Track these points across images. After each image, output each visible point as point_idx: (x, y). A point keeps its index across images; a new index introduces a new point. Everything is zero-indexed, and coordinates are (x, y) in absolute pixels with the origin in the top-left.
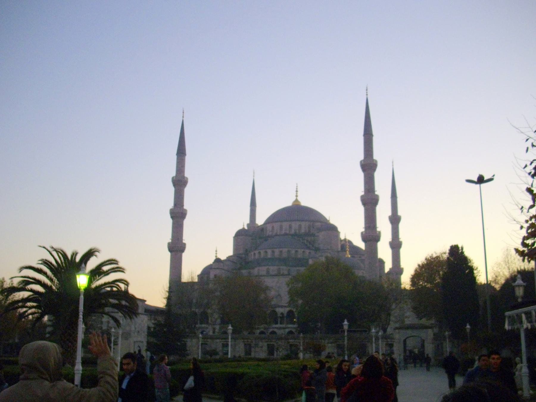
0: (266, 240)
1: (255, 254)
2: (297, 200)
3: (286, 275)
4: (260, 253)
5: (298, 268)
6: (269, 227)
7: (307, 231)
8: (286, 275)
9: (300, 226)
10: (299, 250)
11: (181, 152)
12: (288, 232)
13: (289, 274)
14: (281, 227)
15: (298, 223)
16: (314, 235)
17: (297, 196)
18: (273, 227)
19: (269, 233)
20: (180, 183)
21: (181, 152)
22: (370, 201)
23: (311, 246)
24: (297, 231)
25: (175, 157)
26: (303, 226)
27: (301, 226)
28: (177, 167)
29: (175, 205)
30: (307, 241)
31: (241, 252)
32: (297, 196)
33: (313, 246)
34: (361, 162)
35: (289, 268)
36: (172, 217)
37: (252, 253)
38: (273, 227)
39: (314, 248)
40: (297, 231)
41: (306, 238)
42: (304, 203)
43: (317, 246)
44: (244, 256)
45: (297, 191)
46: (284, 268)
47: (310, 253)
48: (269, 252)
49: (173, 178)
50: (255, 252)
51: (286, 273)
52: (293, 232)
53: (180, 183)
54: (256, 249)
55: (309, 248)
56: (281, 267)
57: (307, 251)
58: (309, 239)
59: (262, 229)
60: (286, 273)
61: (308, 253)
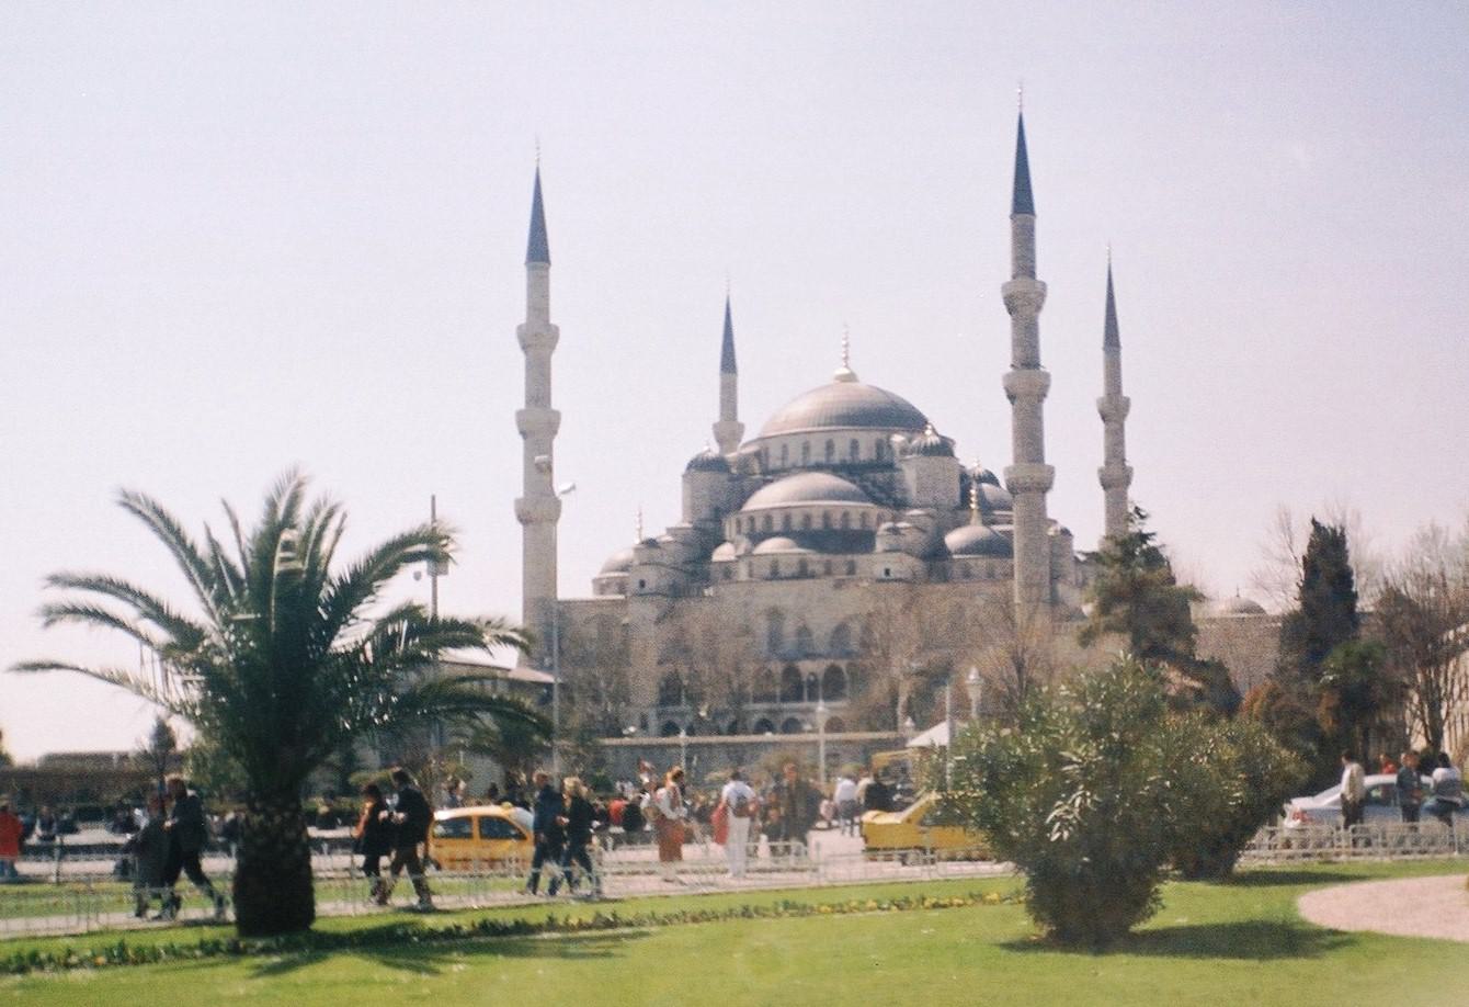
5: (849, 557)
7: (874, 456)
12: (822, 459)
16: (890, 466)
20: (538, 340)
22: (1027, 389)
23: (883, 496)
28: (530, 296)
30: (874, 483)
31: (705, 513)
33: (889, 497)
36: (524, 433)
39: (892, 502)
41: (871, 475)
43: (899, 496)
49: (520, 328)
53: (538, 340)
58: (880, 477)
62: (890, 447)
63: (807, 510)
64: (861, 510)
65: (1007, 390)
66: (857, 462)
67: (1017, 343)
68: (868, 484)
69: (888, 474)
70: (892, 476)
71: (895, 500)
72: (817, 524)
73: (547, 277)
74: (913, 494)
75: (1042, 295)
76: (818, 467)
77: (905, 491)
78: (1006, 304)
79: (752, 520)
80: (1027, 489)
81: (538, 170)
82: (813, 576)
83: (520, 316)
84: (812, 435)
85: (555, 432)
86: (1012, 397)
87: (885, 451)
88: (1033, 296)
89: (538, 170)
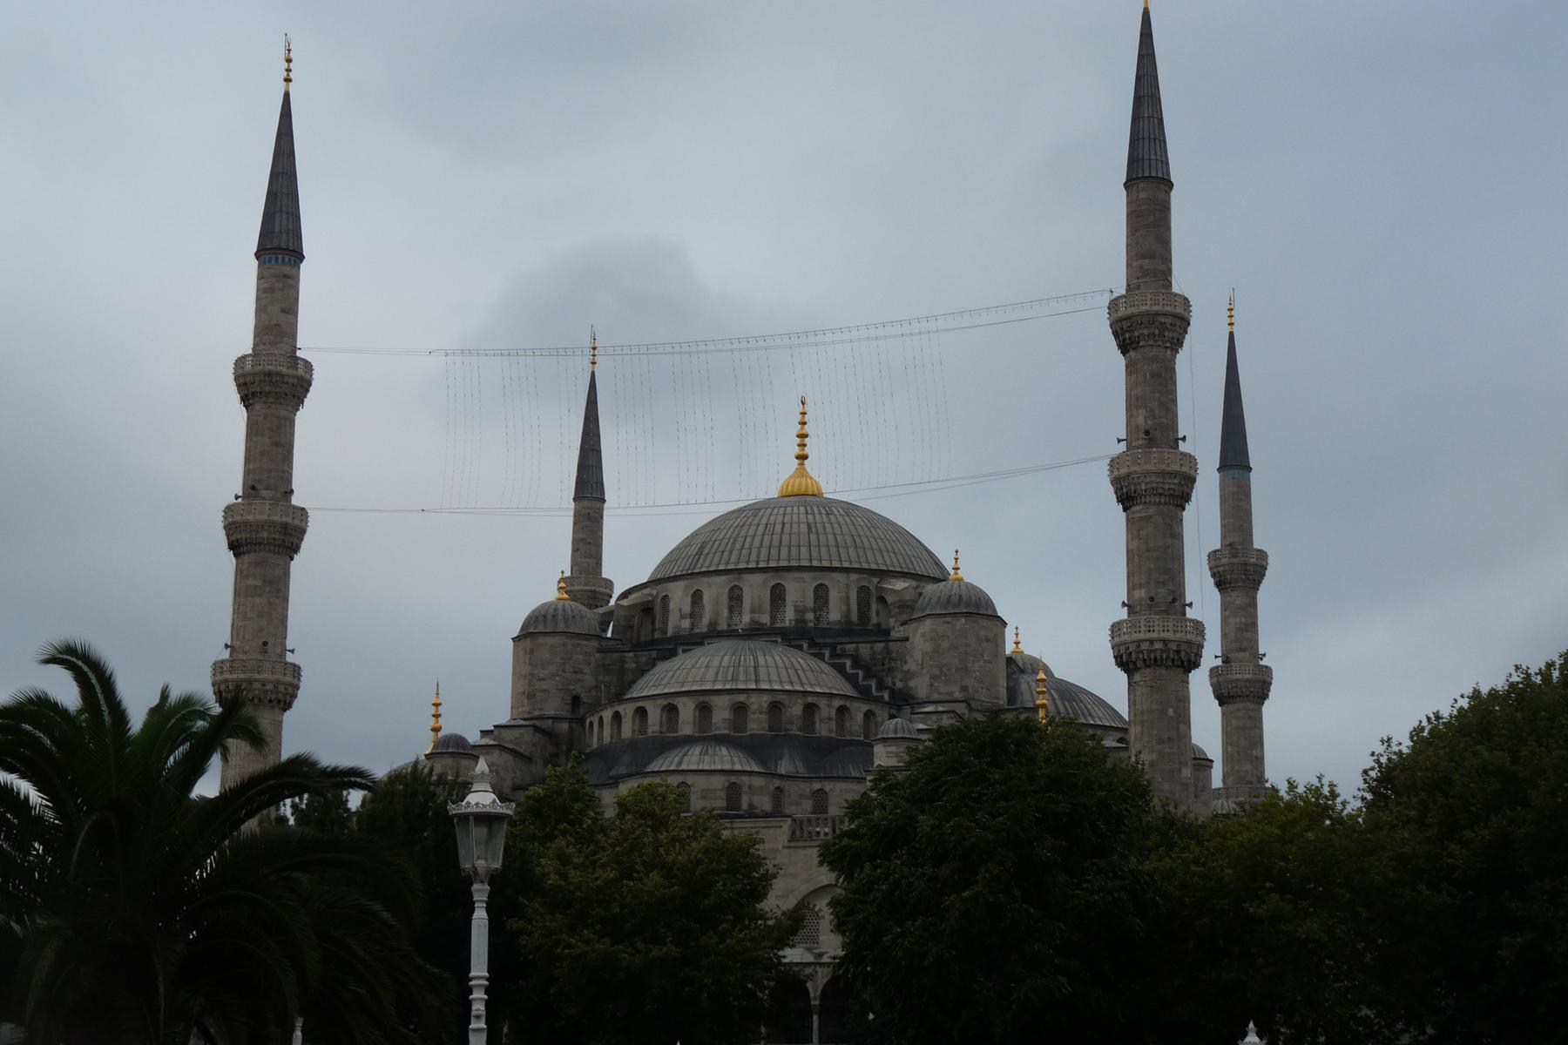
0: (672, 654)
1: (617, 717)
2: (801, 472)
3: (767, 815)
4: (642, 713)
5: (816, 786)
6: (679, 597)
7: (854, 618)
8: (767, 815)
9: (821, 593)
10: (822, 703)
11: (280, 245)
12: (765, 619)
13: (777, 813)
14: (735, 597)
16: (883, 633)
18: (697, 597)
19: (677, 623)
21: (280, 245)
24: (810, 616)
26: (834, 596)
29: (251, 489)
30: (857, 661)
33: (881, 686)
34: (1114, 305)
35: (777, 783)
37: (607, 715)
38: (697, 597)
40: (810, 616)
43: (899, 685)
44: (564, 726)
46: (757, 781)
47: (869, 715)
48: (687, 709)
49: (240, 362)
50: (620, 708)
51: (765, 804)
52: (789, 617)
54: (619, 697)
55: (864, 694)
56: (745, 779)
57: (859, 710)
58: (865, 650)
59: (646, 605)
60: (765, 804)
61: (860, 717)
62: (882, 600)
63: (742, 698)
64: (837, 703)
65: (1117, 483)
66: (823, 625)
67: (1133, 403)
68: (849, 663)
69: (882, 645)
70: (888, 651)
71: (893, 693)
72: (757, 724)
73: (296, 278)
74: (920, 686)
75: (1183, 322)
77: (908, 675)
78: (1116, 334)
80: (1157, 663)
81: (287, 96)
84: (746, 576)
85: (296, 549)
86: (1126, 499)
87: (874, 607)
88: (1168, 321)
89: (287, 96)
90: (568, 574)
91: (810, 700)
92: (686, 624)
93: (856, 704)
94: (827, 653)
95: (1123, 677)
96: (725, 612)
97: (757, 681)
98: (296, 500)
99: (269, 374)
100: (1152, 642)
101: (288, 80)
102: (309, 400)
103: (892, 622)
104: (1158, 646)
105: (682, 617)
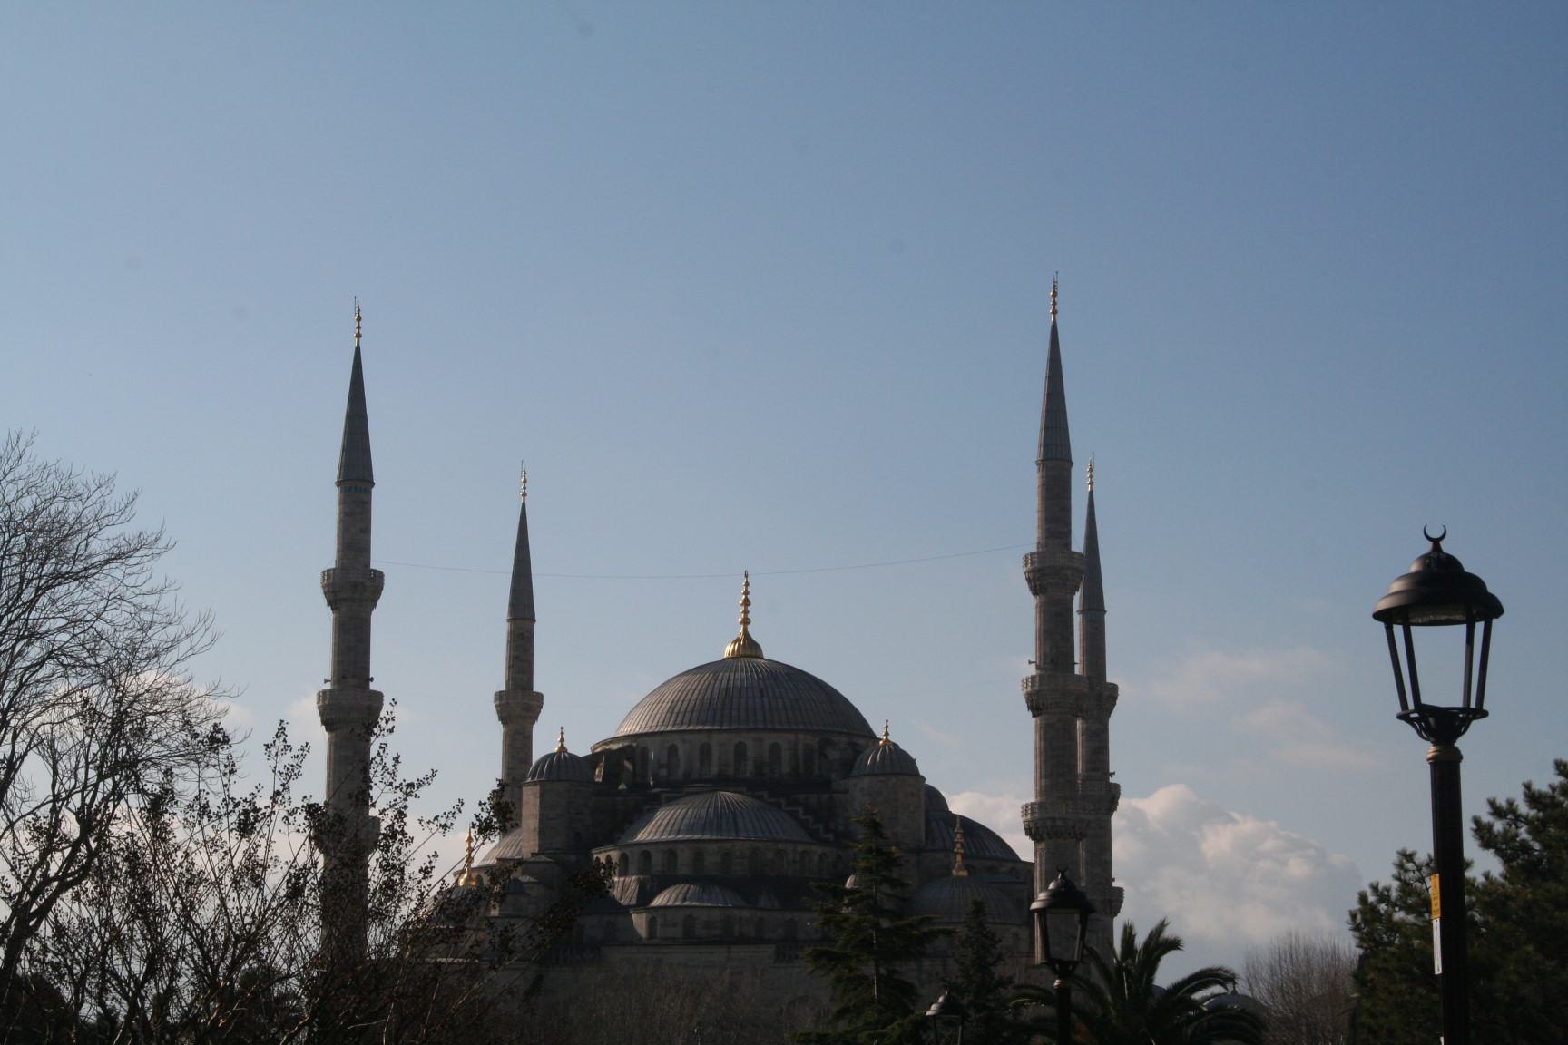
5: (788, 916)
9: (775, 749)
12: (731, 771)
15: (769, 739)
17: (746, 622)
20: (353, 591)
25: (334, 494)
26: (785, 755)
27: (768, 744)
32: (746, 622)
35: (759, 914)
39: (831, 836)
41: (801, 797)
42: (775, 650)
43: (841, 828)
45: (747, 603)
46: (746, 914)
49: (328, 574)
53: (353, 591)
56: (737, 912)
61: (816, 858)
63: (729, 845)
64: (800, 848)
68: (800, 810)
69: (825, 796)
76: (723, 782)
79: (646, 855)
81: (358, 350)
82: (743, 940)
83: (327, 555)
88: (1069, 572)
89: (358, 350)
90: (503, 688)
91: (780, 846)
92: (664, 772)
93: (814, 848)
94: (783, 802)
95: (1031, 843)
96: (697, 764)
97: (737, 831)
98: (373, 686)
99: (355, 585)
100: (1054, 819)
101: (359, 336)
102: (382, 602)
103: (834, 776)
104: (1059, 823)
105: (661, 766)
